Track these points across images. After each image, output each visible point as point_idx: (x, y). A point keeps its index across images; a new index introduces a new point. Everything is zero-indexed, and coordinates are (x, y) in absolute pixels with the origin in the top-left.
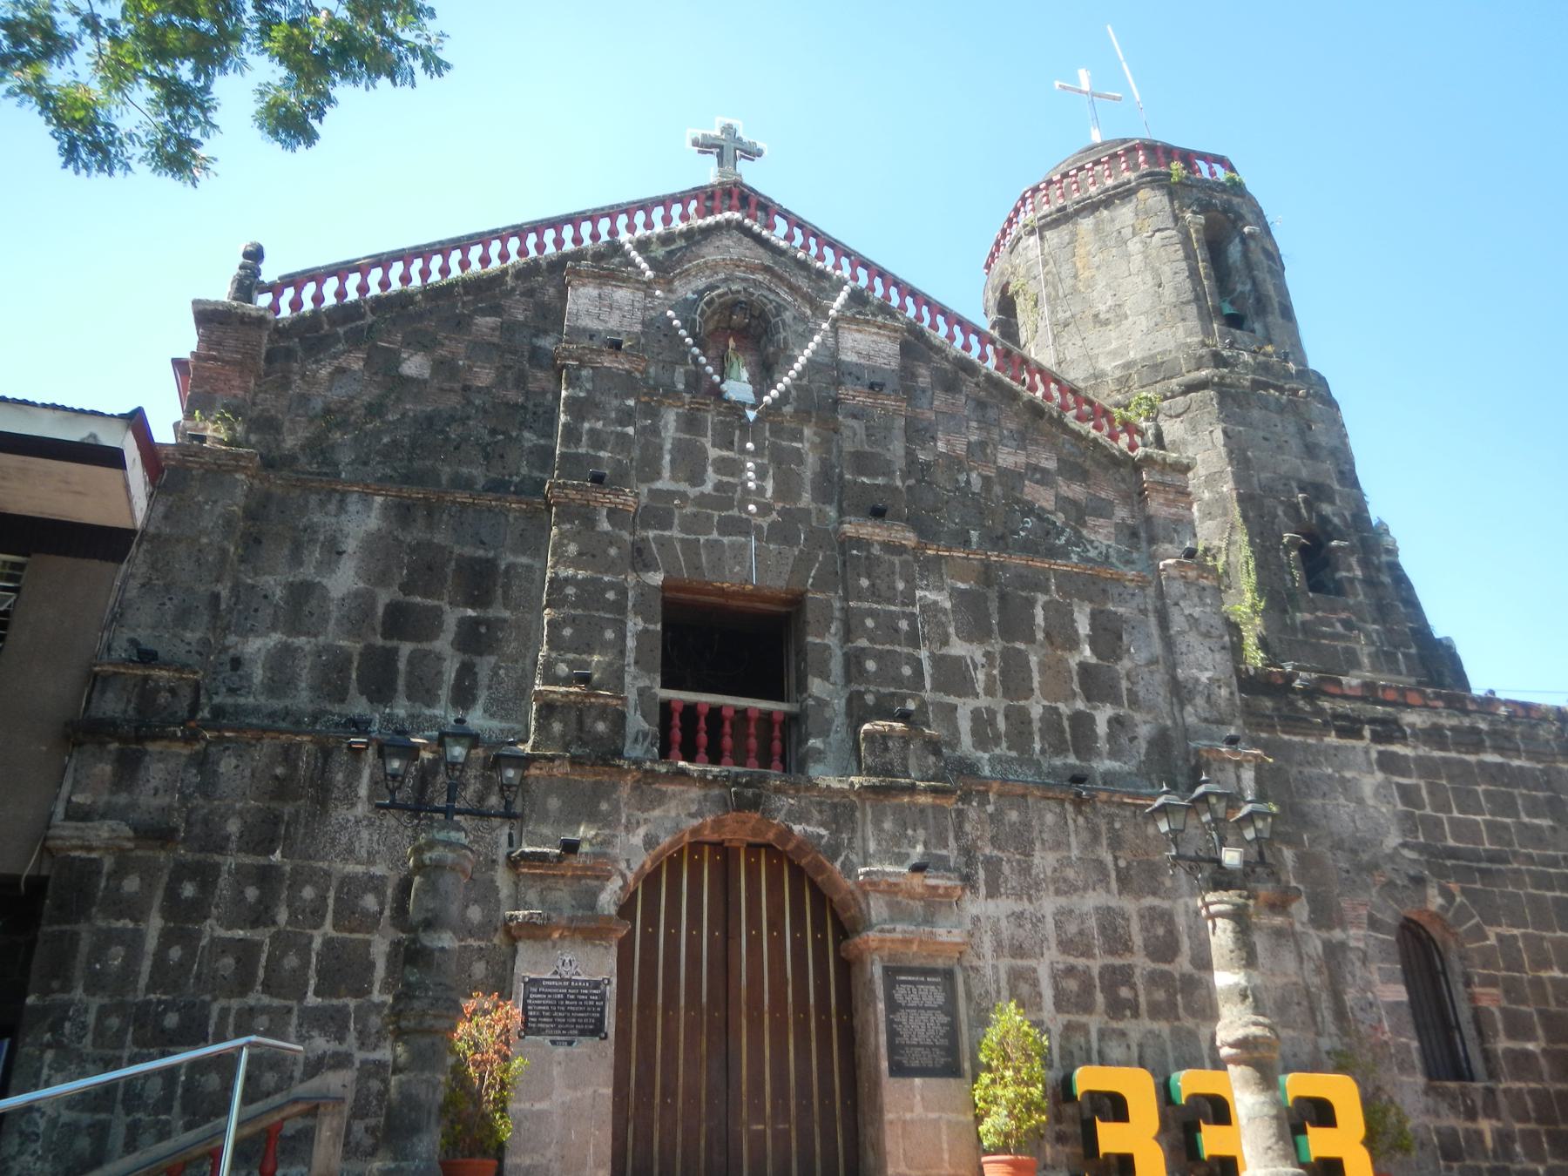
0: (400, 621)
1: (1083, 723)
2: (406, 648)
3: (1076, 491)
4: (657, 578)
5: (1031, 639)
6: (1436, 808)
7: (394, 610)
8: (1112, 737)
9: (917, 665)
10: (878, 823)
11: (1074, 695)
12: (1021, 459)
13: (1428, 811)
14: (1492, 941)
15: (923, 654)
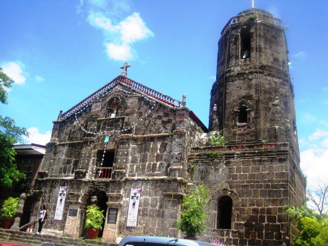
0: (68, 162)
1: (156, 164)
2: (68, 166)
3: (165, 119)
4: (96, 150)
5: (149, 151)
6: (237, 172)
7: (68, 160)
8: (159, 167)
9: (127, 160)
10: (112, 187)
11: (154, 160)
12: (157, 115)
13: (235, 173)
14: (240, 200)
15: (130, 158)
